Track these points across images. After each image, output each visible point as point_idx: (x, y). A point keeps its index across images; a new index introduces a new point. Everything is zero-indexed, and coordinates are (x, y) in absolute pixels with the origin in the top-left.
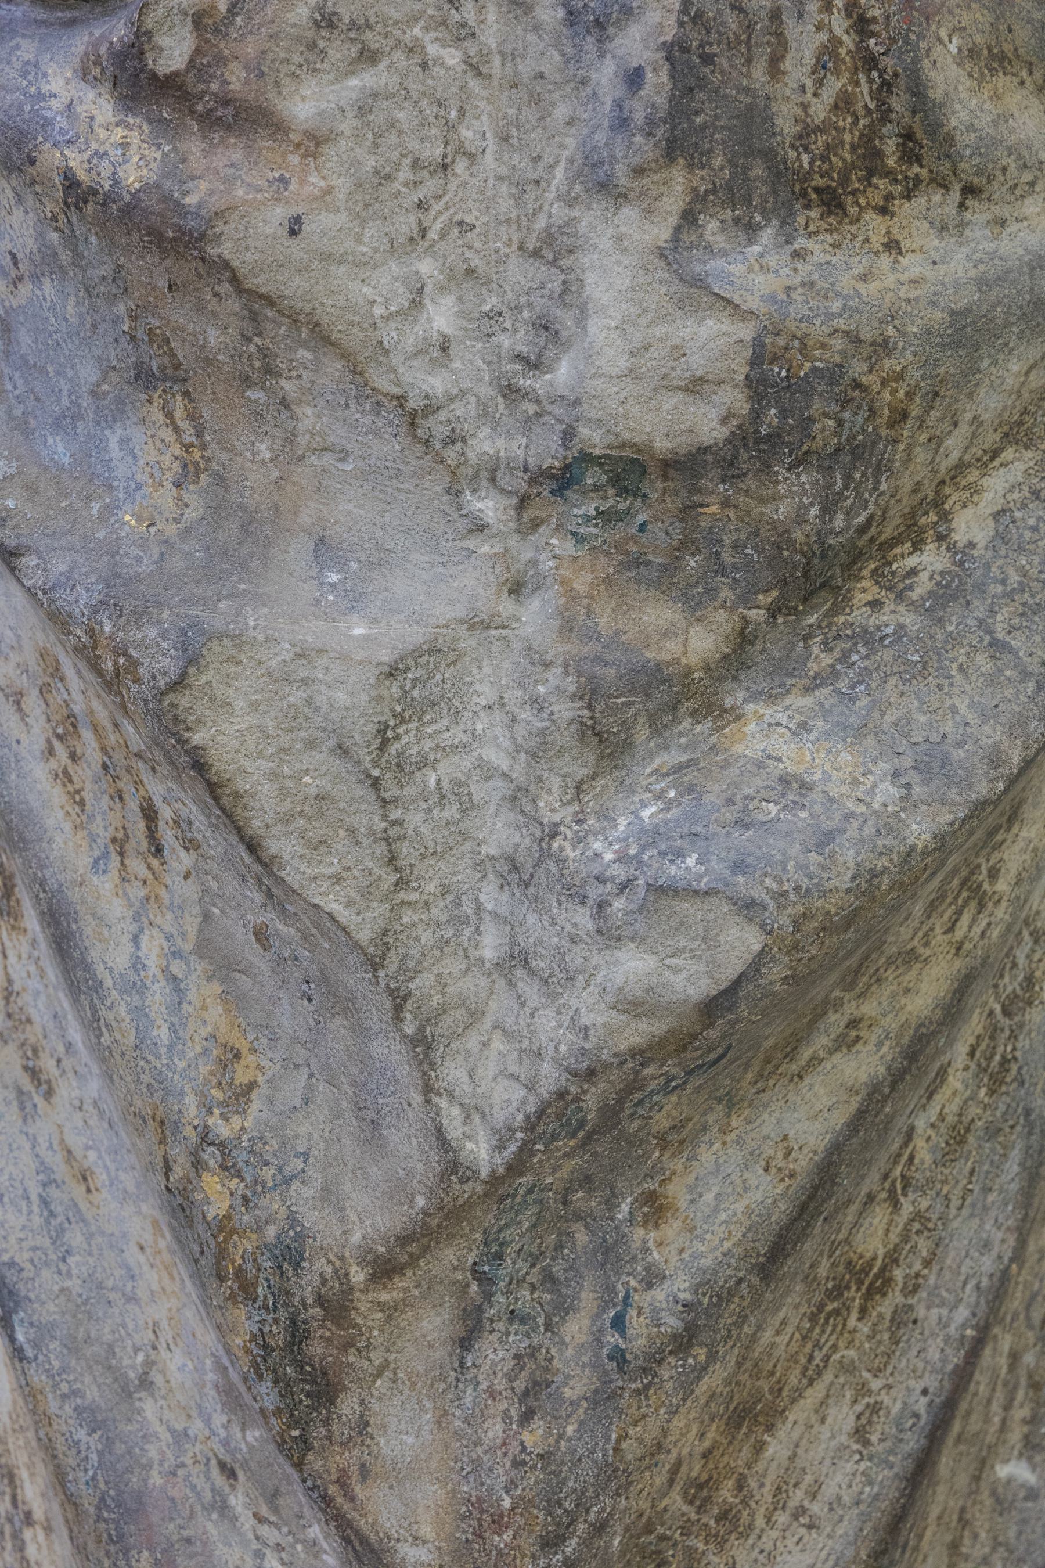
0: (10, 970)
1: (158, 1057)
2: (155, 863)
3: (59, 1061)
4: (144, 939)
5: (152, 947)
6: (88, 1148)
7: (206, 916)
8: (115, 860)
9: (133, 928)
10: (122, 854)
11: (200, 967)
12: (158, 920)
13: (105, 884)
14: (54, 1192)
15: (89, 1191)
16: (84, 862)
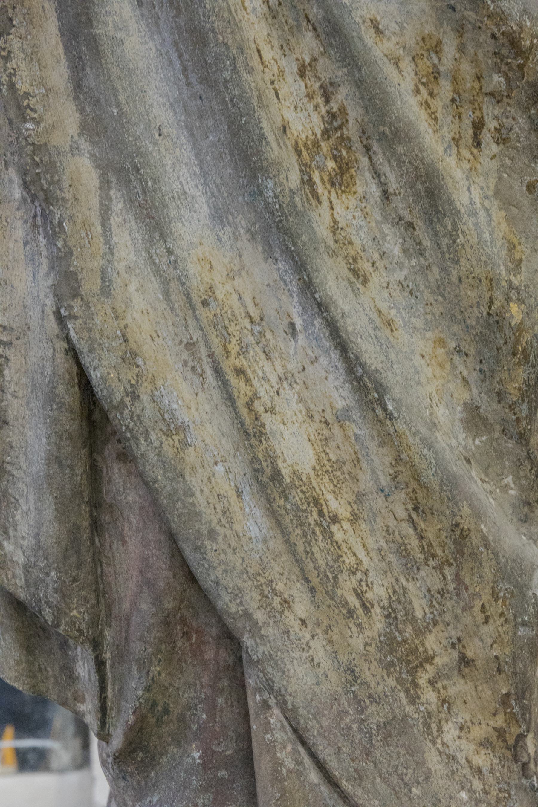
0: (336, 215)
1: (488, 247)
2: (475, 151)
3: (373, 264)
4: (472, 189)
6: (390, 308)
7: (500, 178)
8: (454, 150)
9: (467, 183)
10: (457, 146)
11: (496, 203)
12: (477, 180)
13: (451, 161)
14: (379, 333)
15: (392, 331)
16: (440, 149)
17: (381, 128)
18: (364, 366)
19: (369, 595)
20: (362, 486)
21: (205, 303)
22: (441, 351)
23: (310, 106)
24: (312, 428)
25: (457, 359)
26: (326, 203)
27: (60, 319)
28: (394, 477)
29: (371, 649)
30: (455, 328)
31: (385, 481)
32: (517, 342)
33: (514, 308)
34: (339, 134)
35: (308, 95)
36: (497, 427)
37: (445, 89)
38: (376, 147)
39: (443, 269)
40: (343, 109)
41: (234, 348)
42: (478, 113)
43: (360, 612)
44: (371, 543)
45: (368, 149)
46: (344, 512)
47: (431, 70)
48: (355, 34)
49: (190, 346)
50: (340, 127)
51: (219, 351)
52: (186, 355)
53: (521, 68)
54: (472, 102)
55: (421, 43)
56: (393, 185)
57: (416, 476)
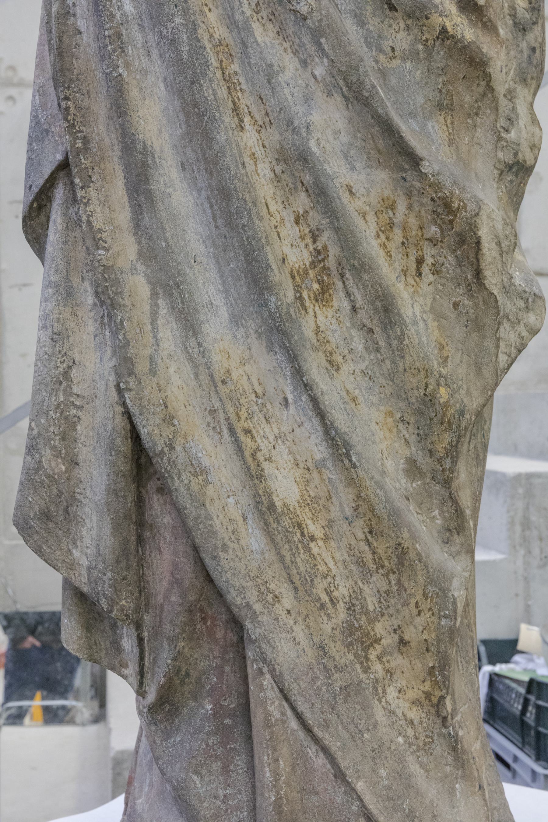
0: (318, 322)
2: (418, 279)
3: (344, 357)
4: (415, 306)
5: (418, 309)
6: (355, 389)
7: (434, 299)
8: (403, 278)
9: (411, 302)
10: (405, 275)
11: (431, 316)
12: (418, 300)
13: (401, 286)
15: (356, 405)
16: (393, 277)
17: (352, 262)
18: (336, 429)
19: (336, 594)
20: (332, 515)
21: (224, 382)
22: (390, 420)
23: (302, 245)
24: (298, 473)
25: (401, 425)
26: (311, 313)
27: (119, 391)
28: (356, 509)
29: (337, 633)
30: (401, 404)
31: (349, 512)
32: (444, 415)
33: (442, 390)
34: (322, 265)
35: (301, 237)
36: (429, 475)
37: (398, 235)
38: (348, 275)
39: (393, 362)
40: (325, 247)
41: (243, 414)
42: (420, 253)
43: (329, 605)
44: (338, 556)
45: (342, 276)
46: (319, 533)
47: (388, 221)
48: (335, 195)
49: (213, 412)
50: (323, 260)
51: (233, 416)
52: (209, 419)
53: (451, 222)
54: (416, 245)
55: (382, 203)
56: (359, 302)
57: (372, 509)
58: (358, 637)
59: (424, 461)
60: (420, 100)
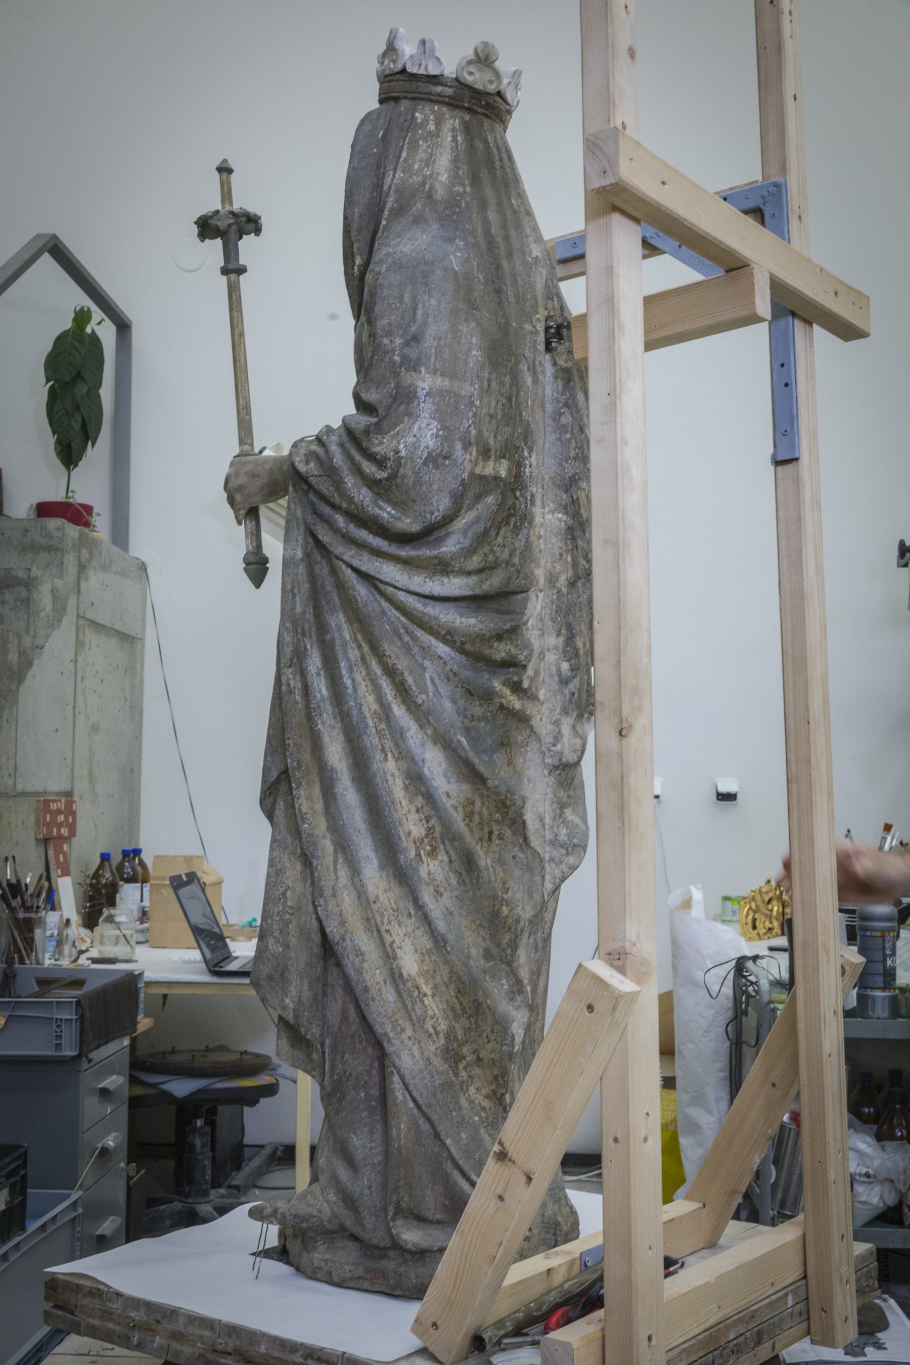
18: (438, 932)
19: (438, 1028)
20: (437, 981)
21: (374, 902)
22: (473, 925)
27: (315, 907)
28: (450, 978)
31: (446, 980)
32: (505, 923)
33: (504, 908)
36: (498, 959)
37: (476, 819)
41: (386, 921)
44: (440, 1006)
46: (429, 992)
49: (368, 920)
51: (379, 923)
52: (366, 923)
57: (459, 978)
58: (452, 1055)
59: (494, 950)
60: (489, 742)
